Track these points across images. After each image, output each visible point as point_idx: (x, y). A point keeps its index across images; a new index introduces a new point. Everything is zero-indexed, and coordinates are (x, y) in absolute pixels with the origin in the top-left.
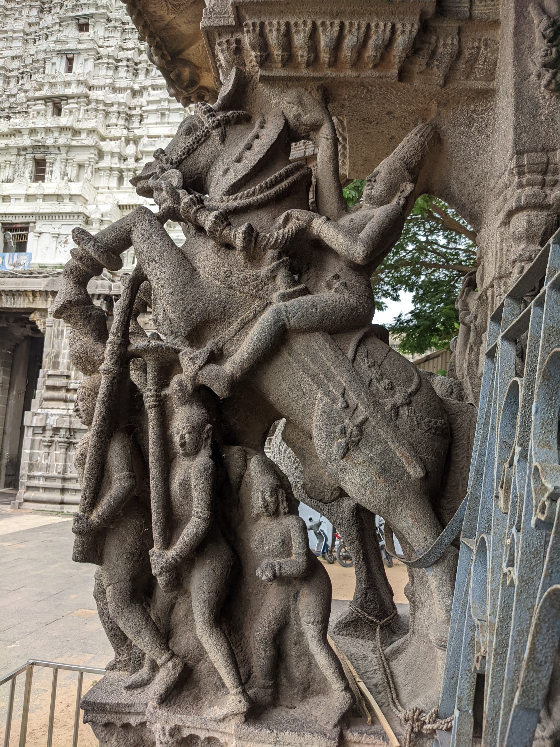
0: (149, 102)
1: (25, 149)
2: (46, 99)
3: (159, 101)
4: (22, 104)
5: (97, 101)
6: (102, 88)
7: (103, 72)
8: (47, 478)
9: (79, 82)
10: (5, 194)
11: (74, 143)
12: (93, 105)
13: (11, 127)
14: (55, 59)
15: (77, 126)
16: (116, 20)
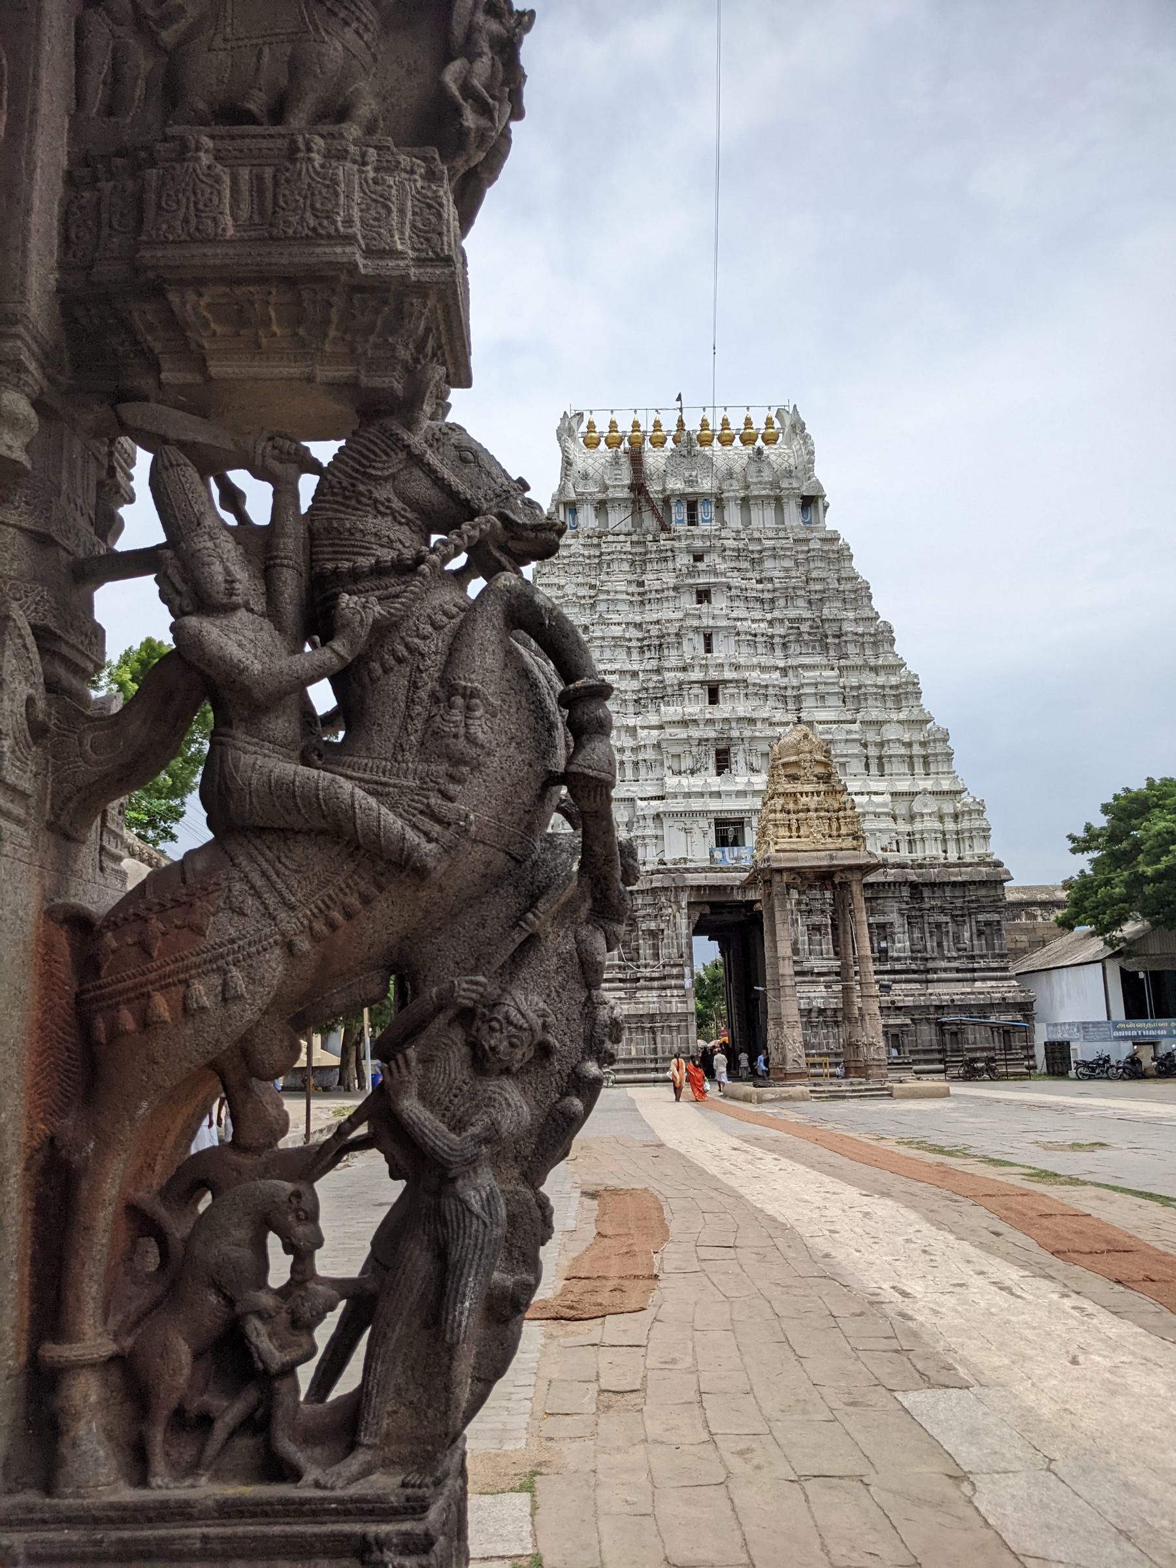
0: (802, 686)
1: (707, 740)
2: (702, 683)
3: (816, 685)
4: (672, 686)
5: (754, 685)
6: (752, 668)
7: (745, 649)
8: (820, 1055)
9: (731, 664)
10: (714, 789)
11: (757, 734)
12: (751, 690)
13: (687, 717)
14: (691, 635)
15: (755, 715)
16: (736, 588)
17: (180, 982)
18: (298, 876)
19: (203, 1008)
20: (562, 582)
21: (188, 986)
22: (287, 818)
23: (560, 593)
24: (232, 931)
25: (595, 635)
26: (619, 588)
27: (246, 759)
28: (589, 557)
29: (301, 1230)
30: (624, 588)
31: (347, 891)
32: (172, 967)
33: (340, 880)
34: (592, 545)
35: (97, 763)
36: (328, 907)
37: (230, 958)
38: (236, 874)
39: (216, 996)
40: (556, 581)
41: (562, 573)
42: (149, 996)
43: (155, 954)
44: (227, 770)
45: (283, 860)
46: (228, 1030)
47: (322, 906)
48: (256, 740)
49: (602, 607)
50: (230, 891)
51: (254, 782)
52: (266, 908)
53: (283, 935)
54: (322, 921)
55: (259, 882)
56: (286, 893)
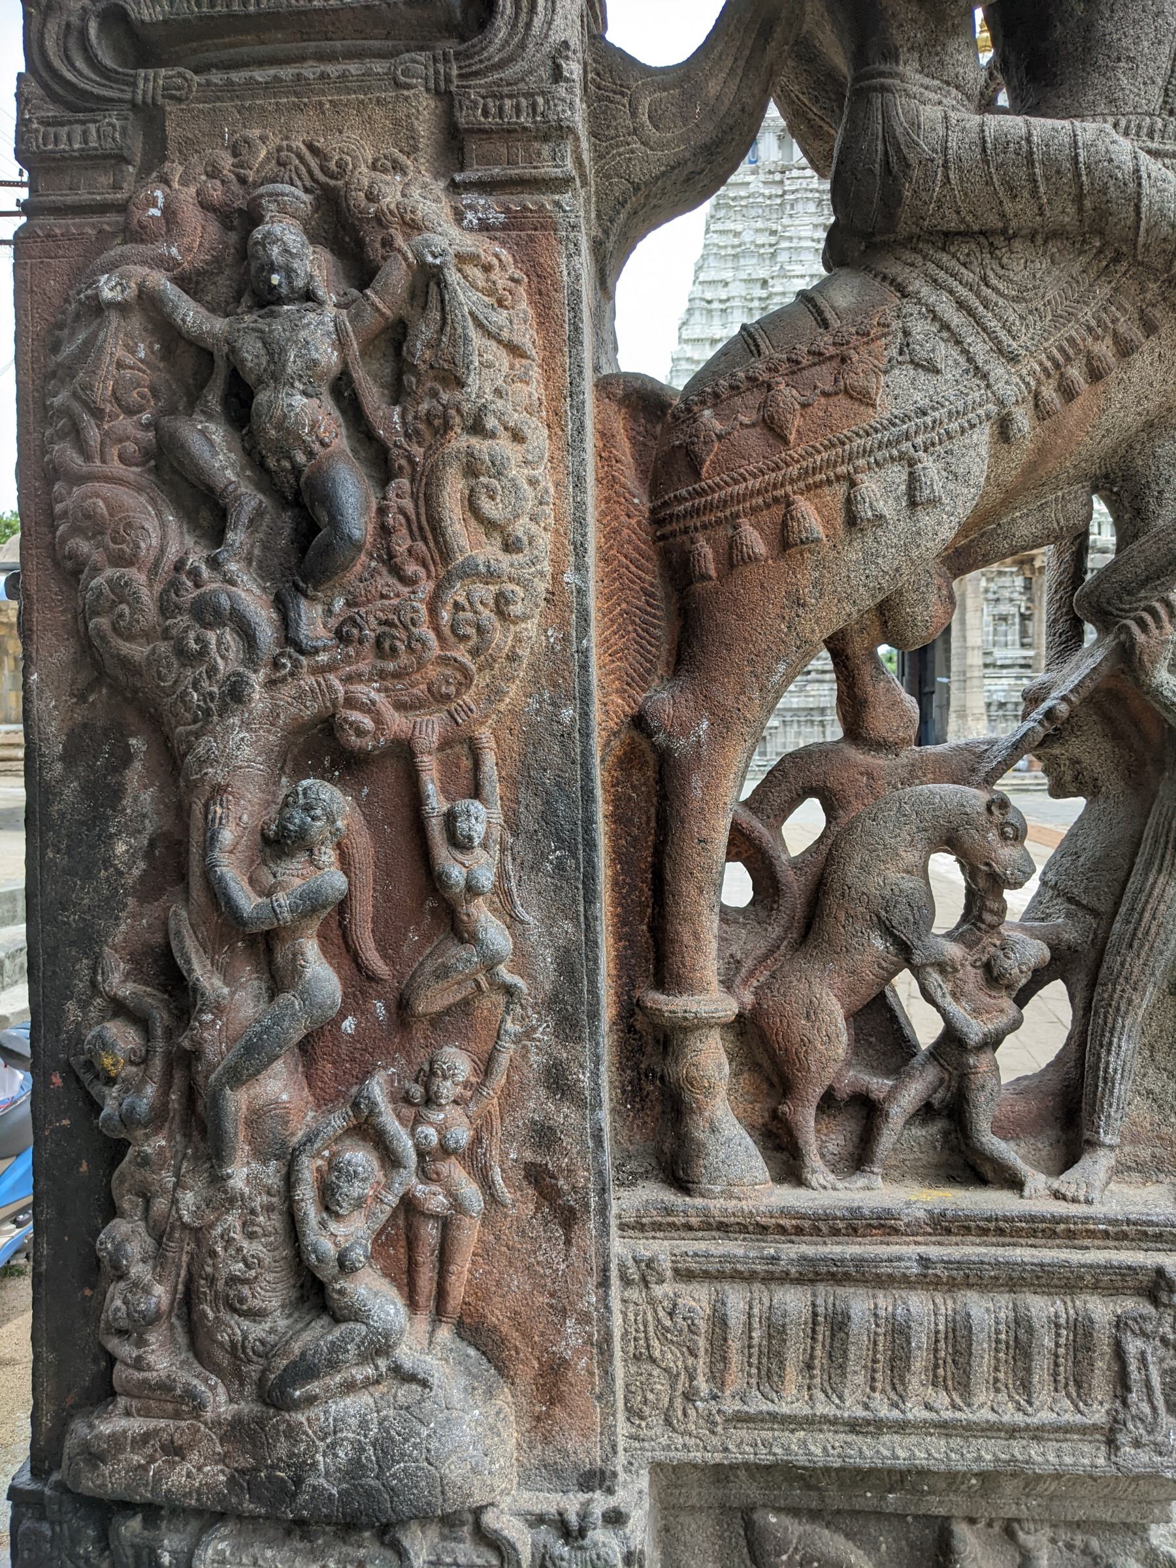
17: (838, 478)
18: (1021, 307)
19: (881, 517)
20: (739, 228)
21: (853, 484)
22: (1008, 206)
23: (736, 241)
24: (918, 396)
25: (774, 290)
26: (803, 234)
27: (930, 114)
28: (770, 197)
29: (1006, 853)
30: (809, 234)
31: (1099, 331)
32: (825, 455)
33: (1087, 314)
34: (774, 182)
35: (662, 146)
36: (1068, 359)
37: (919, 440)
38: (910, 308)
39: (897, 499)
40: (732, 226)
41: (739, 217)
42: (789, 504)
43: (792, 437)
44: (899, 131)
45: (994, 281)
46: (915, 554)
47: (1058, 356)
48: (936, 82)
49: (783, 257)
50: (906, 333)
51: (953, 144)
52: (970, 360)
53: (1001, 403)
54: (1053, 383)
55: (956, 319)
56: (1002, 334)
